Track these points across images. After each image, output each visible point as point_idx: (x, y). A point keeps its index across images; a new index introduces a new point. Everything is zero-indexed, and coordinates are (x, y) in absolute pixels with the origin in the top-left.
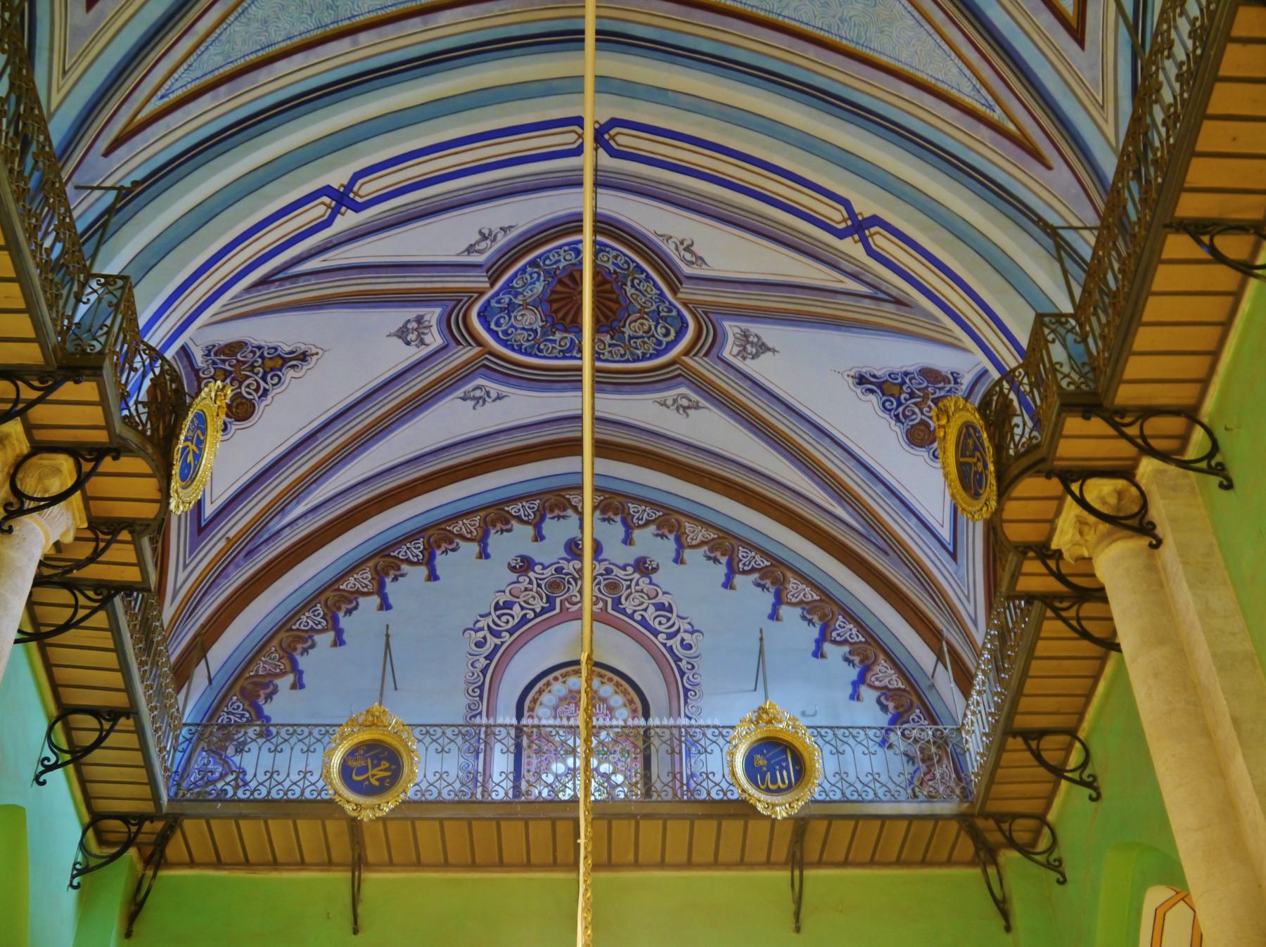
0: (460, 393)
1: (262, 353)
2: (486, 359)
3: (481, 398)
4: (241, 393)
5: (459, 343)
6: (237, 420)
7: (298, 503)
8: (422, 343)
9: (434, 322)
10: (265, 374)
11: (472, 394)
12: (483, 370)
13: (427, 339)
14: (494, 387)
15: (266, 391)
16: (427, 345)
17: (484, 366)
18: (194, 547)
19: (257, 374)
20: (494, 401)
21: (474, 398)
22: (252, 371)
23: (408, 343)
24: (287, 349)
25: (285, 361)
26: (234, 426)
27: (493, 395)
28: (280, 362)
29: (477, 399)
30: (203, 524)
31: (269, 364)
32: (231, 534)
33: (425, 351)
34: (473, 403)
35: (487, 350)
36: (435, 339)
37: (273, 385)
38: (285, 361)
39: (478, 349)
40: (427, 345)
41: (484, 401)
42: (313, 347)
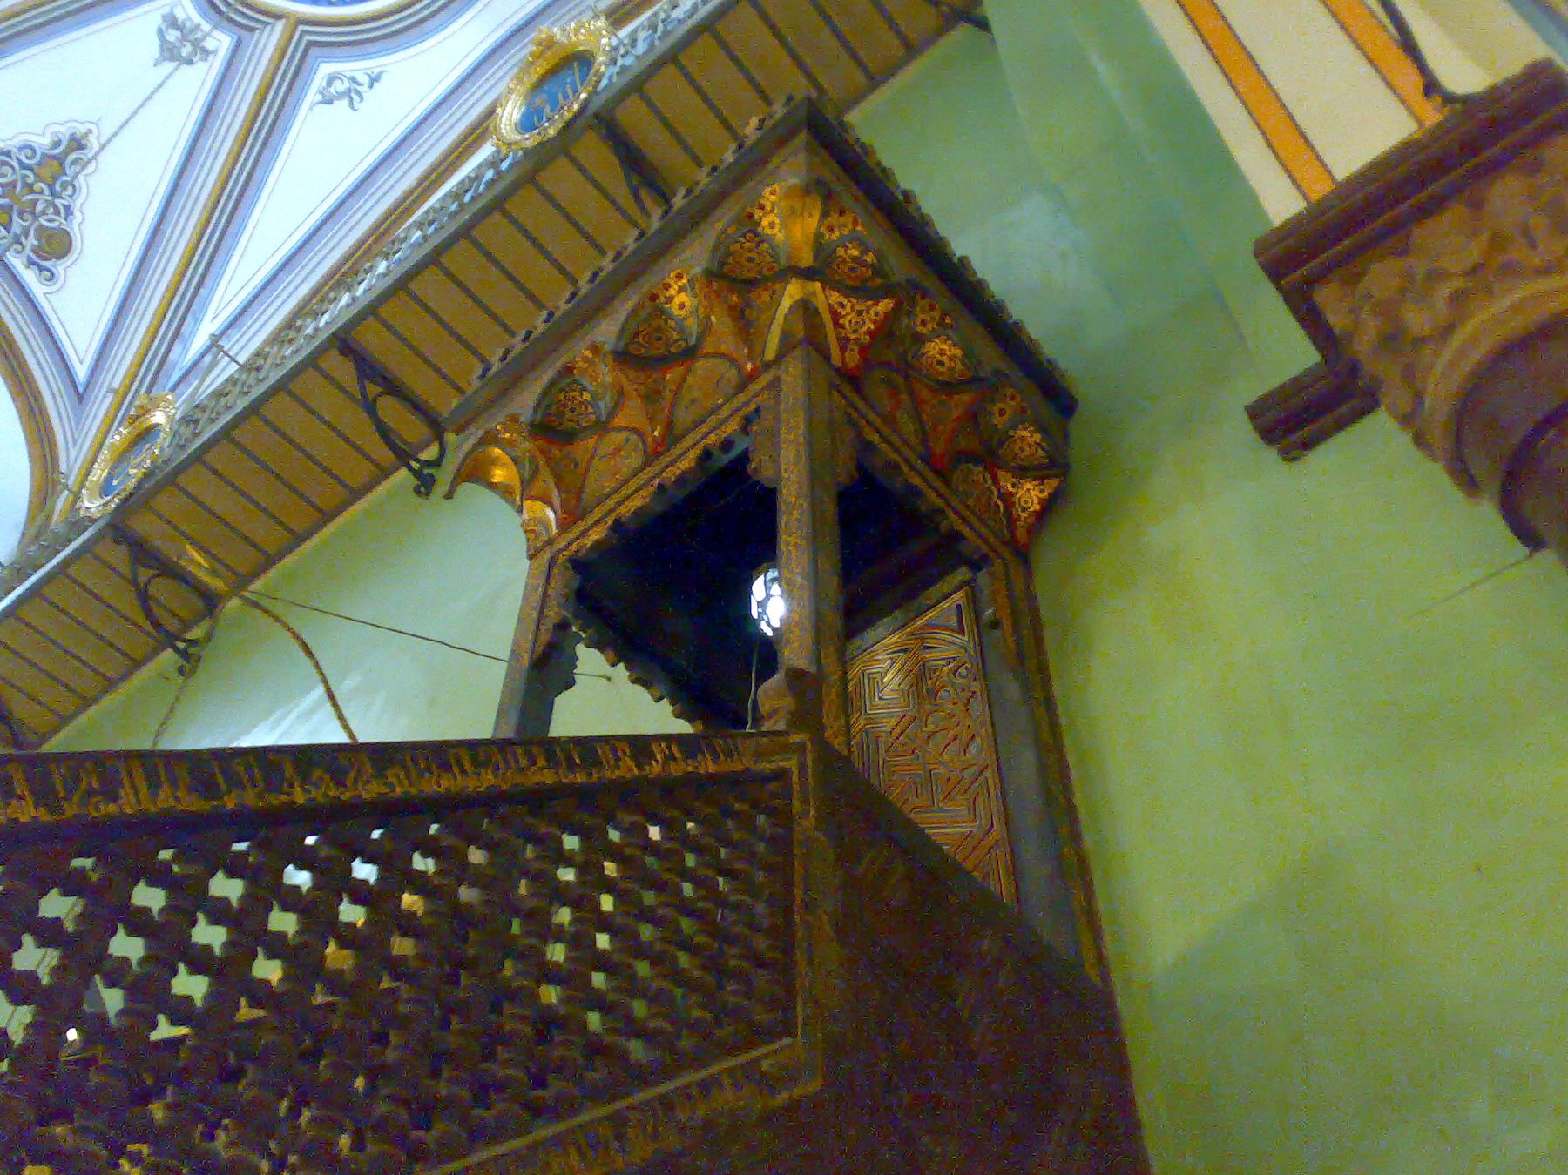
0: (312, 95)
1: (20, 162)
2: (304, 33)
3: (349, 90)
4: (42, 225)
5: (251, 30)
6: (58, 258)
7: (198, 321)
8: (206, 53)
9: (197, 18)
10: (51, 187)
11: (332, 90)
12: (314, 52)
13: (209, 44)
14: (358, 68)
15: (67, 208)
16: (215, 52)
17: (310, 44)
18: (79, 419)
19: (42, 193)
20: (371, 86)
21: (340, 96)
22: (32, 191)
23: (190, 62)
24: (46, 141)
25: (60, 159)
26: (60, 267)
27: (365, 80)
28: (55, 163)
29: (347, 94)
30: (81, 390)
31: (46, 172)
32: (116, 385)
33: (218, 62)
34: (345, 102)
35: (292, 20)
36: (221, 42)
37: (71, 196)
38: (60, 159)
39: (280, 25)
40: (215, 52)
41: (358, 93)
42: (78, 126)
